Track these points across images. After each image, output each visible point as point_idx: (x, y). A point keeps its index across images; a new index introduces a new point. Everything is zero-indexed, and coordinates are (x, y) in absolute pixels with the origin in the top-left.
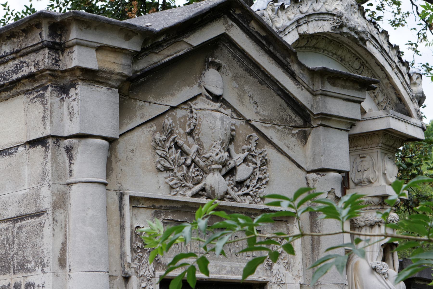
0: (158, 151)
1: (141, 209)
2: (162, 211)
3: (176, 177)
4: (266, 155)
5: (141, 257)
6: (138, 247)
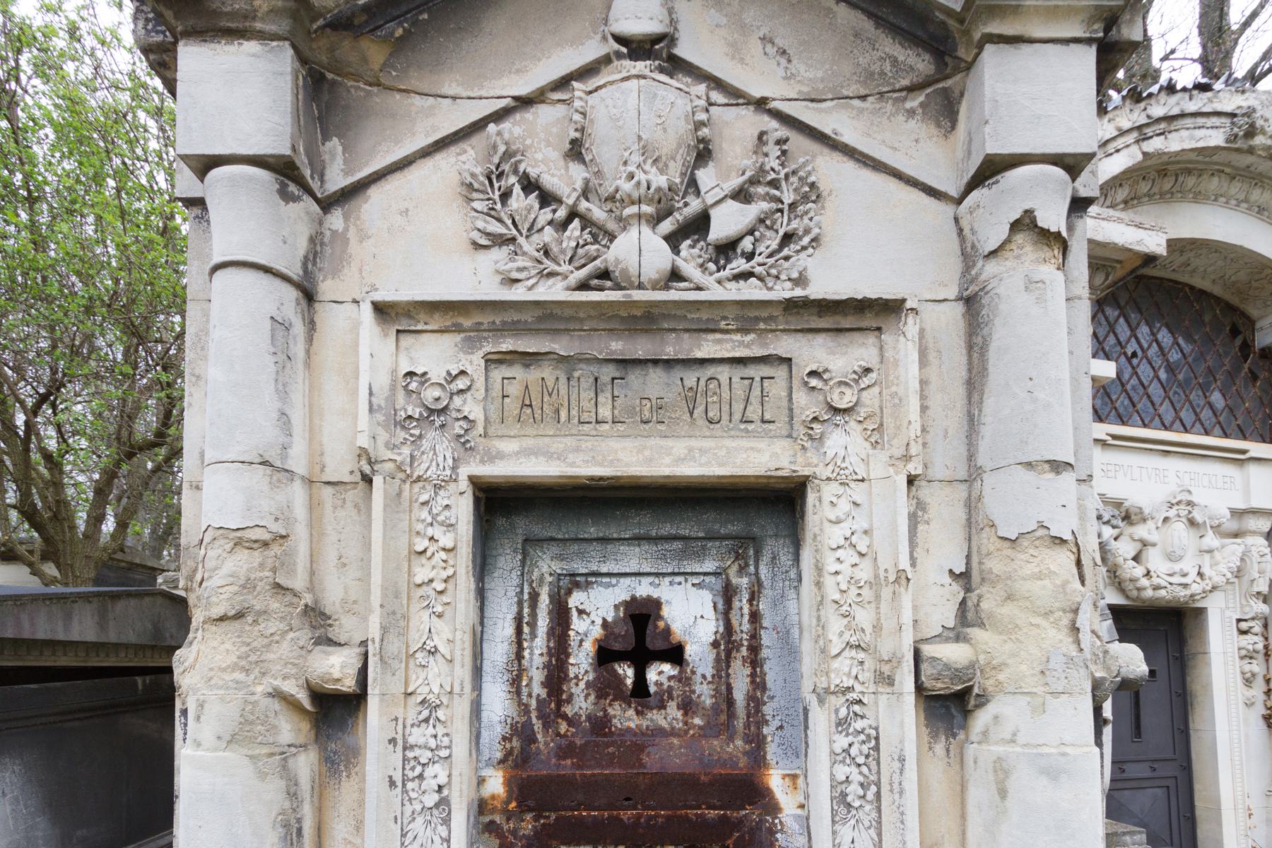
0: (476, 205)
1: (425, 336)
2: (485, 334)
3: (524, 254)
4: (809, 173)
5: (420, 437)
6: (410, 417)
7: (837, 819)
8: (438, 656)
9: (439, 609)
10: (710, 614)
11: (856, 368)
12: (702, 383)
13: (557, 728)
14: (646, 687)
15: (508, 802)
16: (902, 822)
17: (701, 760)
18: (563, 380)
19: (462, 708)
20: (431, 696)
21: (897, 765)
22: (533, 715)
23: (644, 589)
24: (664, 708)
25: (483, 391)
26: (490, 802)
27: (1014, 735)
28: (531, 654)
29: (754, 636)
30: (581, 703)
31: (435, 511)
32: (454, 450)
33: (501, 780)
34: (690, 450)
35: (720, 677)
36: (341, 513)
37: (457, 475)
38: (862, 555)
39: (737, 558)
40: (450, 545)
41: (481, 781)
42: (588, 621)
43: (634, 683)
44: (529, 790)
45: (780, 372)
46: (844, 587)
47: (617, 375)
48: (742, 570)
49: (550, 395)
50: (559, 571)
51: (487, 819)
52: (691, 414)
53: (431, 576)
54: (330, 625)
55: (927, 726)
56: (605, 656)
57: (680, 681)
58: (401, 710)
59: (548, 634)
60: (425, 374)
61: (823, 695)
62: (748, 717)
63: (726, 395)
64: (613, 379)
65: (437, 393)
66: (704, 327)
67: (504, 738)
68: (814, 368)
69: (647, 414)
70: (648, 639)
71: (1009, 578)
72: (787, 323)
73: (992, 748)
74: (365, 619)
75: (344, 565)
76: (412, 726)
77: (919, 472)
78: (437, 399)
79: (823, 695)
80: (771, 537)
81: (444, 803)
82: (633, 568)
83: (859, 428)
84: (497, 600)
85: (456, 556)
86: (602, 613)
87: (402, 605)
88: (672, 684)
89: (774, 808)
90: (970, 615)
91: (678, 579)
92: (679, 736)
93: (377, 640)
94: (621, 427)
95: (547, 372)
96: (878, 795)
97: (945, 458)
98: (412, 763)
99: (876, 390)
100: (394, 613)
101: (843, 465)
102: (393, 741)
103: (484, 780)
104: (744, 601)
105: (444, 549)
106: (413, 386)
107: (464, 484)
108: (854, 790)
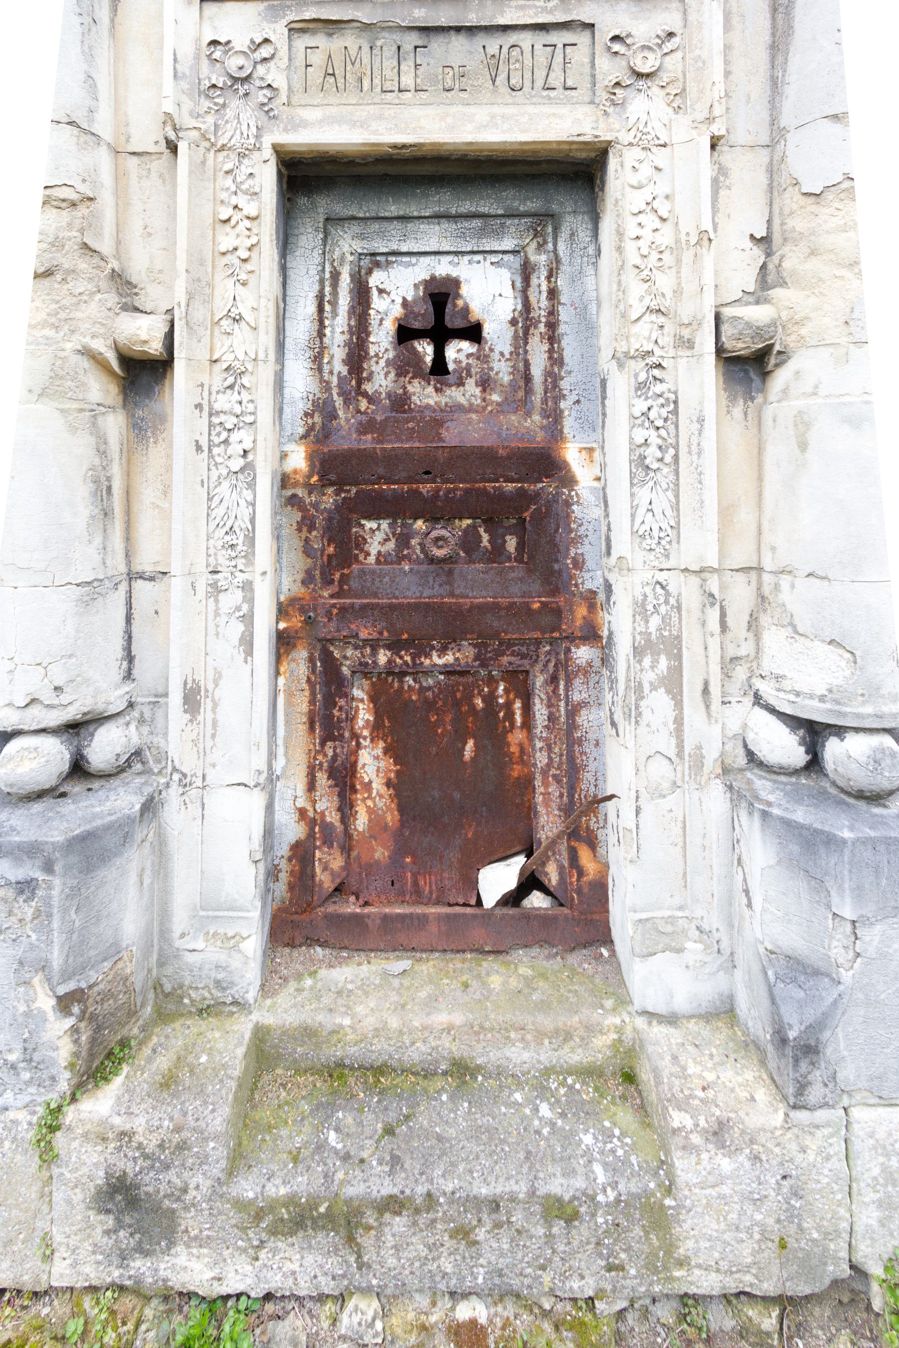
5: (224, 106)
6: (214, 86)
7: (635, 481)
8: (243, 323)
9: (243, 276)
10: (508, 291)
11: (660, 33)
12: (505, 50)
13: (357, 406)
14: (445, 364)
15: (310, 476)
16: (700, 482)
17: (499, 435)
19: (266, 374)
20: (236, 362)
21: (696, 426)
22: (335, 392)
23: (443, 268)
24: (463, 384)
25: (286, 60)
26: (292, 476)
27: (816, 387)
28: (333, 332)
29: (552, 313)
30: (381, 380)
31: (239, 179)
32: (257, 119)
33: (303, 455)
34: (493, 117)
35: (518, 354)
37: (261, 143)
38: (663, 220)
39: (535, 236)
40: (254, 214)
41: (284, 456)
42: (389, 300)
44: (331, 467)
45: (583, 39)
46: (644, 251)
47: (420, 43)
48: (540, 247)
49: (353, 64)
50: (360, 251)
51: (289, 493)
52: (494, 82)
53: (235, 244)
54: (136, 294)
55: (725, 390)
56: (405, 334)
57: (478, 358)
58: (207, 376)
59: (349, 312)
60: (229, 42)
61: (621, 360)
62: (546, 393)
63: (528, 62)
64: (416, 47)
65: (241, 61)
67: (306, 414)
69: (449, 83)
70: (447, 318)
71: (813, 233)
73: (792, 403)
74: (171, 288)
75: (150, 235)
76: (218, 392)
77: (723, 132)
78: (241, 68)
79: (621, 360)
80: (569, 213)
81: (248, 468)
82: (433, 246)
83: (662, 93)
84: (299, 278)
85: (260, 224)
86: (402, 292)
87: (207, 273)
88: (470, 361)
89: (569, 481)
90: (770, 279)
91: (477, 257)
92: (477, 412)
93: (183, 304)
95: (350, 40)
96: (676, 457)
97: (748, 125)
98: (218, 429)
99: (678, 55)
100: (199, 280)
101: (645, 130)
102: (199, 406)
103: (286, 455)
104: (543, 278)
105: (248, 218)
106: (217, 55)
107: (268, 153)
108: (652, 452)
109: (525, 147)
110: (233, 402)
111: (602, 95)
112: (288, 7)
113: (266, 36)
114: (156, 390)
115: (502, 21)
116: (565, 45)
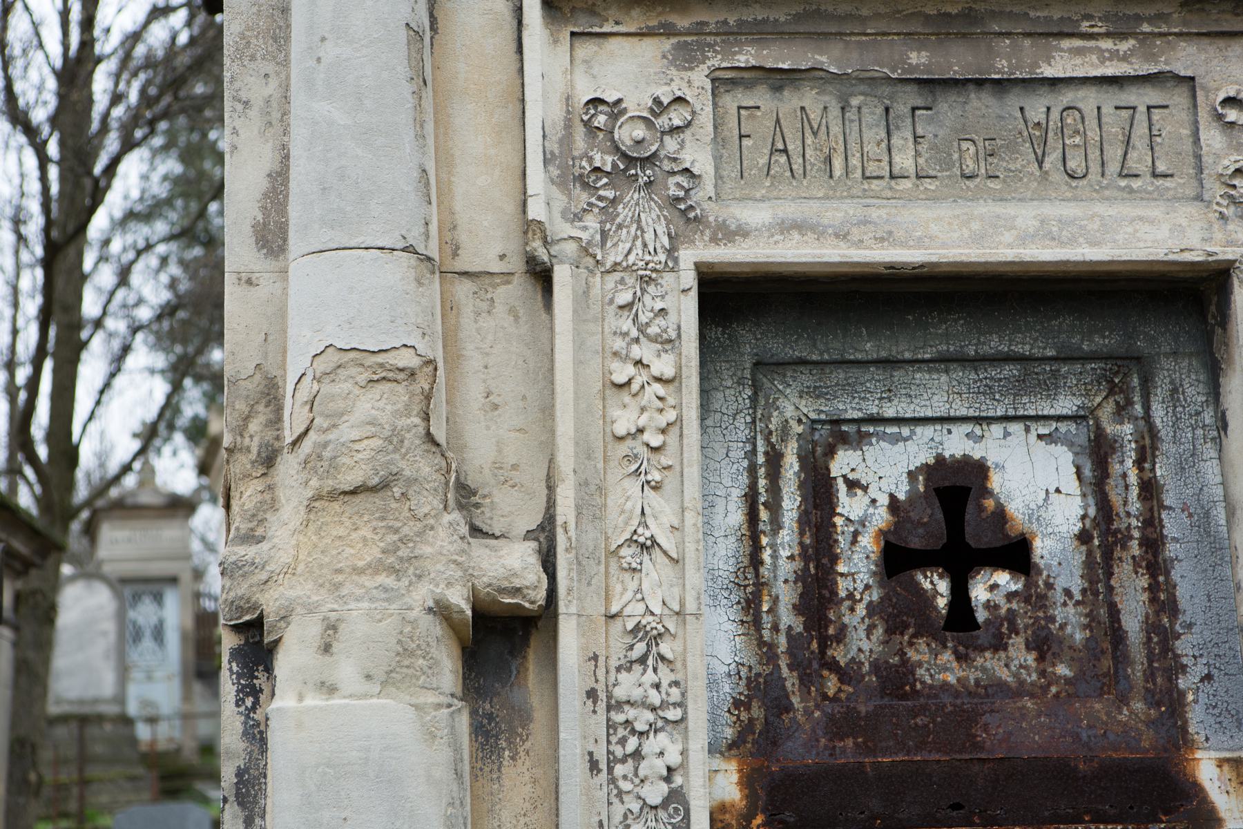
1: (613, 43)
2: (709, 39)
5: (614, 202)
6: (597, 169)
8: (657, 553)
9: (655, 476)
12: (1055, 115)
18: (835, 111)
25: (711, 129)
31: (643, 319)
36: (487, 323)
37: (676, 260)
40: (669, 372)
43: (951, 605)
45: (1178, 98)
47: (919, 102)
49: (815, 134)
54: (477, 506)
60: (619, 101)
65: (640, 132)
66: (1055, 30)
68: (1232, 94)
69: (970, 165)
72: (1185, 24)
75: (496, 407)
76: (618, 669)
81: (676, 798)
85: (680, 390)
94: (930, 185)
95: (810, 99)
98: (621, 732)
100: (587, 484)
105: (658, 380)
106: (601, 120)
107: (689, 279)
109: (1098, 269)
110: (647, 686)
111: (1215, 190)
112: (710, 45)
113: (679, 94)
114: (513, 668)
115: (1049, 72)
116: (1149, 108)
